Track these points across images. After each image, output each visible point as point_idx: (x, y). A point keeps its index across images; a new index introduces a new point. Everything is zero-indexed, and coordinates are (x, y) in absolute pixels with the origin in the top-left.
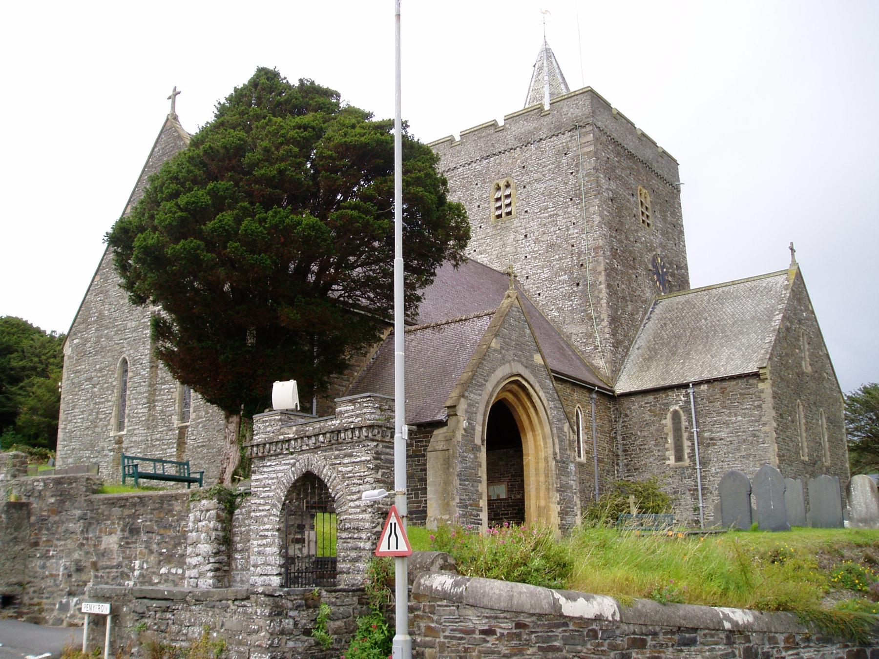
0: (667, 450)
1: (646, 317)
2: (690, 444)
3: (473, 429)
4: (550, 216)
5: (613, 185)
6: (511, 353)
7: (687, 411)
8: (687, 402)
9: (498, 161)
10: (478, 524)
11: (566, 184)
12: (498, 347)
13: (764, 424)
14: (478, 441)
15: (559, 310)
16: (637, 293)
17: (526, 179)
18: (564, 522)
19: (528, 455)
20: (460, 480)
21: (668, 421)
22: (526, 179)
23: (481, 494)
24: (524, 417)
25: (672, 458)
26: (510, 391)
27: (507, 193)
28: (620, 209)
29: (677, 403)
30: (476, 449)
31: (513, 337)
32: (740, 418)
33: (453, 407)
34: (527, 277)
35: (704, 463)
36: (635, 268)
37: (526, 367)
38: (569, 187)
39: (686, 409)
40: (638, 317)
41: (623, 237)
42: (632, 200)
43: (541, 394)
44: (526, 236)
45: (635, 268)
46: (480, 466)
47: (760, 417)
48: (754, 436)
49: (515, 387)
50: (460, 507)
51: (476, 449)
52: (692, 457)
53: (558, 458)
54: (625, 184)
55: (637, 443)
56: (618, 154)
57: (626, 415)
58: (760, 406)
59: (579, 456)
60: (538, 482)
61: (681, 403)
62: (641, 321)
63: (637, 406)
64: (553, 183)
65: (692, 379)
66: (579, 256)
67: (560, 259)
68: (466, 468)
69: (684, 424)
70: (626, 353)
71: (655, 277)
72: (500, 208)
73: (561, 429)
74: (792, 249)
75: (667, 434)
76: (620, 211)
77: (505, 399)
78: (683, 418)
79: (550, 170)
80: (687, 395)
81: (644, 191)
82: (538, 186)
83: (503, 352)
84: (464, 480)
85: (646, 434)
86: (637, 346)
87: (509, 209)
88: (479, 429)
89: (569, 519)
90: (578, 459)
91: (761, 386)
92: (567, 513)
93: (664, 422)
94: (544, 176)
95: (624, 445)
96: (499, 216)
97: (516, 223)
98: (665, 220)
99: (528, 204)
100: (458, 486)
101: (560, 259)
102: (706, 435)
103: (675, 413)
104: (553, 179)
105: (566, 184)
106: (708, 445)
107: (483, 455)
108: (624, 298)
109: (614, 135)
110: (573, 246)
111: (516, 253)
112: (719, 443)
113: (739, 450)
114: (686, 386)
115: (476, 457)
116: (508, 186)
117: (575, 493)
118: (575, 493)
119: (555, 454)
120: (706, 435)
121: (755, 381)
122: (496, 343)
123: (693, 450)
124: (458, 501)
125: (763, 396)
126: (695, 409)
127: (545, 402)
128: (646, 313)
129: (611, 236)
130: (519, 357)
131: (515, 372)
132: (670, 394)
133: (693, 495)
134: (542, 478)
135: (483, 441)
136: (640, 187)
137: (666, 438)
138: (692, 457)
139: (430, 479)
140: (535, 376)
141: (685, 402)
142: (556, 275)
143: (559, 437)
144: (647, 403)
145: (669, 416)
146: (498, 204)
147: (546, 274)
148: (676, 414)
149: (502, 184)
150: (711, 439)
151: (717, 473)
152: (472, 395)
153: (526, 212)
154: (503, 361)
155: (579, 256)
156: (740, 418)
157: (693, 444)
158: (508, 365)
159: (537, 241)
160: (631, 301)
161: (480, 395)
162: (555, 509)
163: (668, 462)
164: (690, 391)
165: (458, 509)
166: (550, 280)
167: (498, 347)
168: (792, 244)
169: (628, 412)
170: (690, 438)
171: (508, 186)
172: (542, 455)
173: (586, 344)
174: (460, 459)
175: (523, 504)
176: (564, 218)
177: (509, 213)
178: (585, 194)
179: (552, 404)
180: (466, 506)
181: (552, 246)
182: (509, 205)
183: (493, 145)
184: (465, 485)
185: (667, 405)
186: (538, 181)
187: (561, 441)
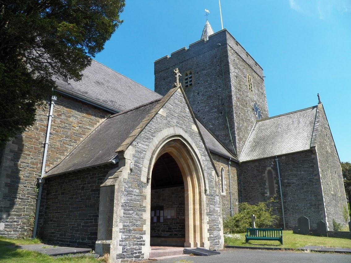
0: (266, 189)
1: (252, 129)
2: (277, 186)
3: (140, 170)
4: (209, 84)
5: (237, 71)
6: (175, 121)
7: (276, 170)
8: (275, 165)
9: (186, 64)
10: (141, 245)
11: (215, 70)
12: (165, 115)
13: (316, 175)
14: (144, 179)
15: (213, 124)
16: (248, 118)
17: (198, 70)
18: (212, 236)
19: (188, 190)
20: (124, 209)
21: (266, 175)
22: (198, 70)
23: (145, 221)
24: (185, 166)
25: (268, 193)
26: (174, 147)
27: (190, 76)
28: (240, 81)
29: (270, 166)
30: (141, 185)
31: (177, 111)
32: (302, 172)
33: (122, 152)
34: (199, 111)
35: (285, 195)
36: (247, 107)
37: (186, 132)
38: (217, 71)
39: (275, 168)
40: (249, 128)
41: (241, 93)
42: (245, 79)
43: (196, 150)
44: (198, 94)
45: (247, 107)
46: (145, 199)
47: (313, 171)
48: (311, 181)
49: (178, 145)
50: (123, 232)
51: (141, 185)
52: (278, 192)
53: (208, 192)
54: (243, 73)
55: (251, 185)
56: (238, 59)
57: (245, 172)
58: (313, 166)
59: (223, 192)
60: (194, 209)
61: (272, 166)
62: (250, 130)
63: (250, 168)
64: (209, 70)
65: (278, 154)
66: (222, 100)
67: (213, 102)
68: (131, 200)
69: (274, 176)
70: (244, 144)
71: (256, 112)
72: (187, 83)
73: (211, 175)
74: (318, 96)
75: (265, 181)
76: (240, 82)
77: (171, 152)
78: (273, 172)
79: (208, 65)
80: (275, 162)
81: (250, 77)
82: (203, 72)
83: (169, 119)
84: (128, 210)
85: (255, 181)
86: (249, 141)
87: (191, 83)
88: (145, 171)
89: (215, 233)
90: (222, 194)
91: (313, 156)
92: (214, 230)
93: (264, 175)
94: (206, 67)
95: (244, 186)
96: (187, 86)
97: (194, 88)
98: (258, 90)
99: (199, 80)
100: (122, 215)
101: (213, 102)
102: (286, 181)
103: (269, 172)
104: (210, 68)
105: (215, 70)
106: (286, 186)
107: (148, 191)
108: (242, 119)
109: (236, 51)
110: (219, 96)
111: (194, 101)
112: (292, 185)
113: (303, 188)
114: (274, 157)
115: (141, 192)
116: (191, 73)
117: (220, 216)
118: (220, 216)
119: (206, 190)
120: (286, 181)
121: (310, 154)
122: (163, 112)
123: (279, 187)
124: (121, 227)
125: (314, 161)
126: (280, 168)
127: (200, 157)
128: (252, 127)
129: (236, 92)
130: (181, 124)
131: (177, 133)
132: (266, 161)
133: (279, 211)
134: (197, 206)
135: (148, 179)
136: (248, 75)
137: (265, 183)
138: (278, 192)
139: (101, 209)
140: (193, 139)
141: (274, 165)
142: (212, 109)
143: (209, 179)
144: (254, 166)
145: (266, 172)
146: (187, 81)
147: (207, 109)
148: (269, 172)
149: (188, 72)
150: (288, 183)
151: (292, 200)
152: (140, 145)
153: (198, 83)
154: (168, 125)
155: (222, 100)
156: (302, 172)
157: (279, 186)
158: (172, 128)
159: (203, 95)
160: (246, 121)
161: (147, 145)
162: (206, 227)
163: (266, 195)
164: (277, 159)
165: (121, 234)
166: (209, 112)
167: (165, 115)
168: (318, 94)
169: (246, 171)
170: (278, 183)
171: (191, 73)
172: (197, 191)
173: (225, 140)
174: (125, 193)
175: (184, 223)
176: (215, 84)
177: (191, 85)
178: (224, 73)
179: (204, 158)
180: (130, 231)
181: (210, 97)
182: (191, 81)
183: (184, 57)
184: (129, 214)
185: (265, 167)
186: (203, 70)
187: (210, 182)
